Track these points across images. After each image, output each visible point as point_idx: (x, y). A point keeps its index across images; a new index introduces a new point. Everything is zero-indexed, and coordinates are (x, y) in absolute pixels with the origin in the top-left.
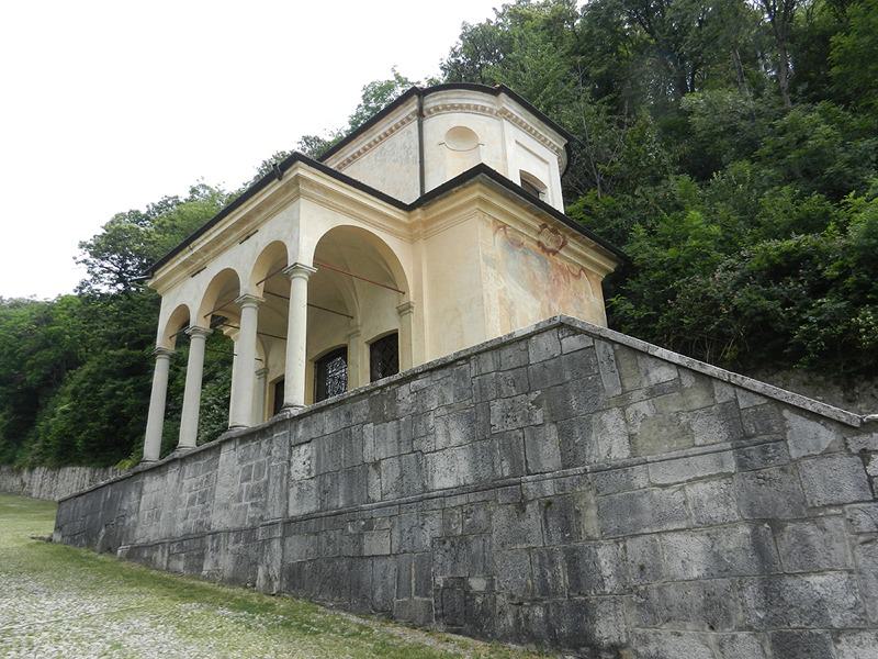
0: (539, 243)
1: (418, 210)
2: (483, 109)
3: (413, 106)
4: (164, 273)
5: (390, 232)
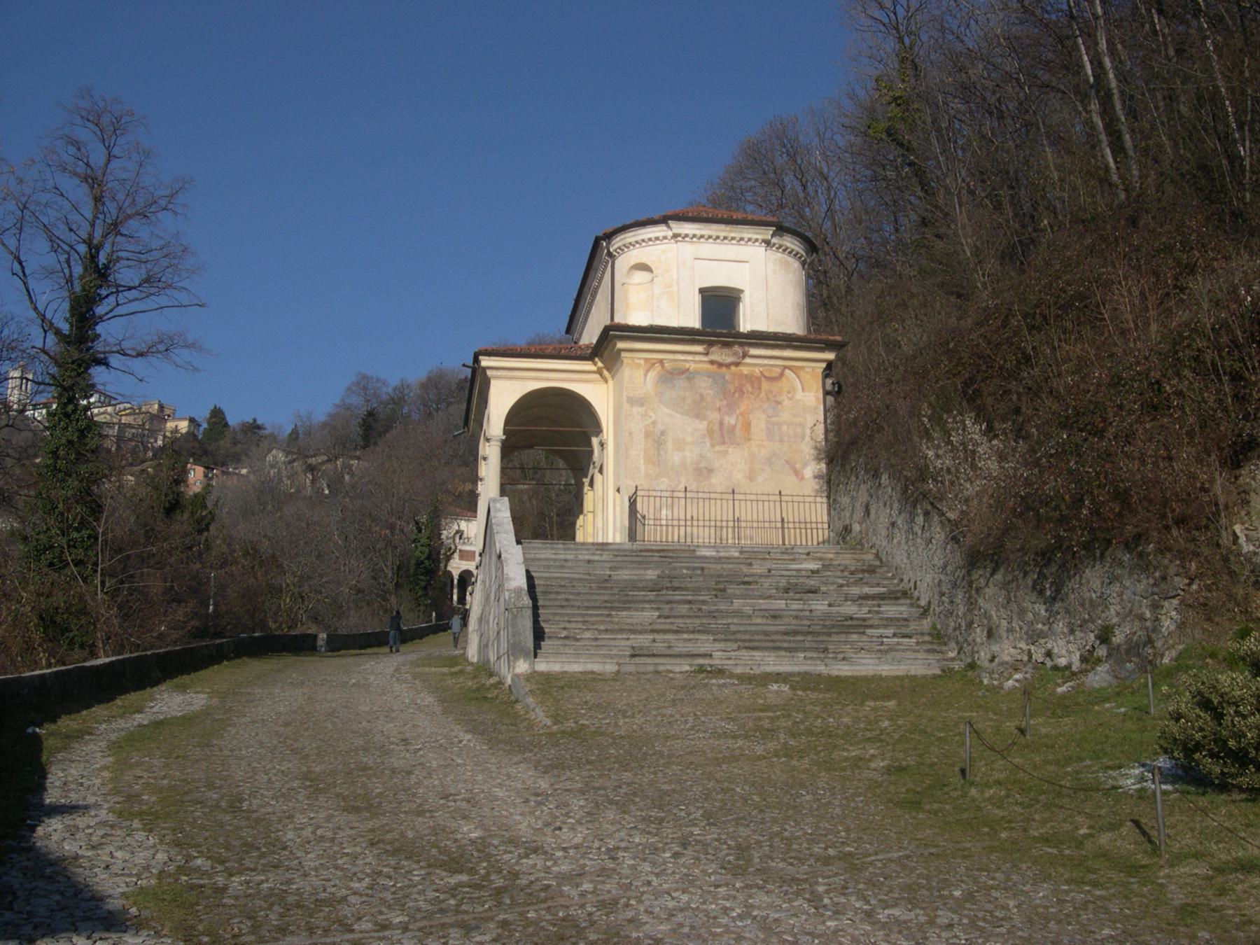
0: (712, 362)
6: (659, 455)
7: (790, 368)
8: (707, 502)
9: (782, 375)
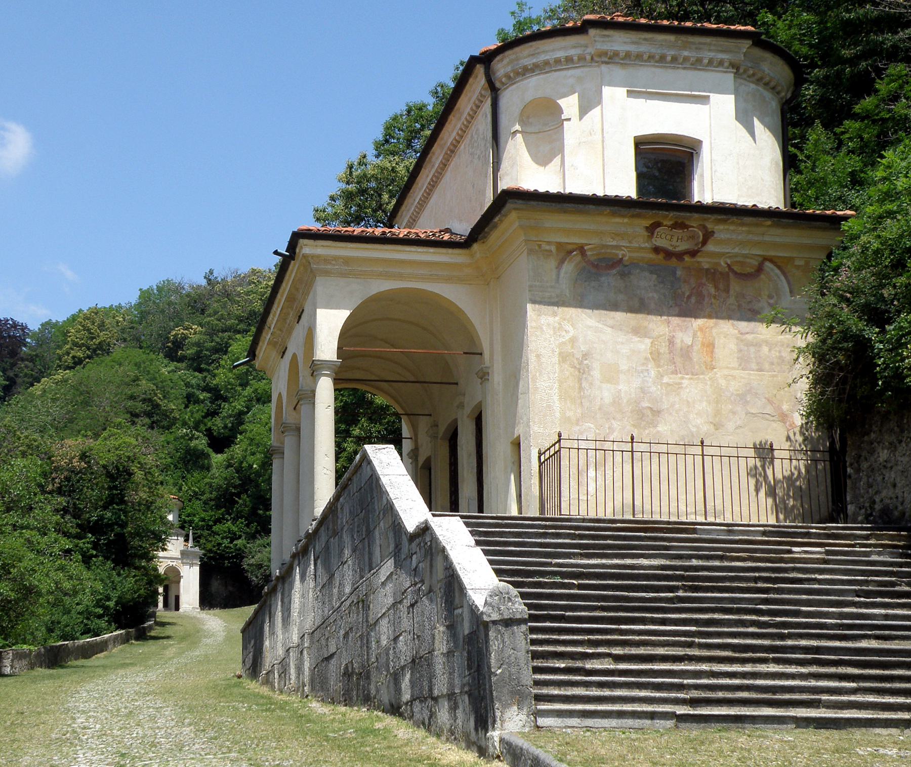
1: (475, 246)
2: (569, 60)
3: (478, 82)
5: (449, 280)
7: (771, 260)
8: (664, 458)
9: (760, 269)
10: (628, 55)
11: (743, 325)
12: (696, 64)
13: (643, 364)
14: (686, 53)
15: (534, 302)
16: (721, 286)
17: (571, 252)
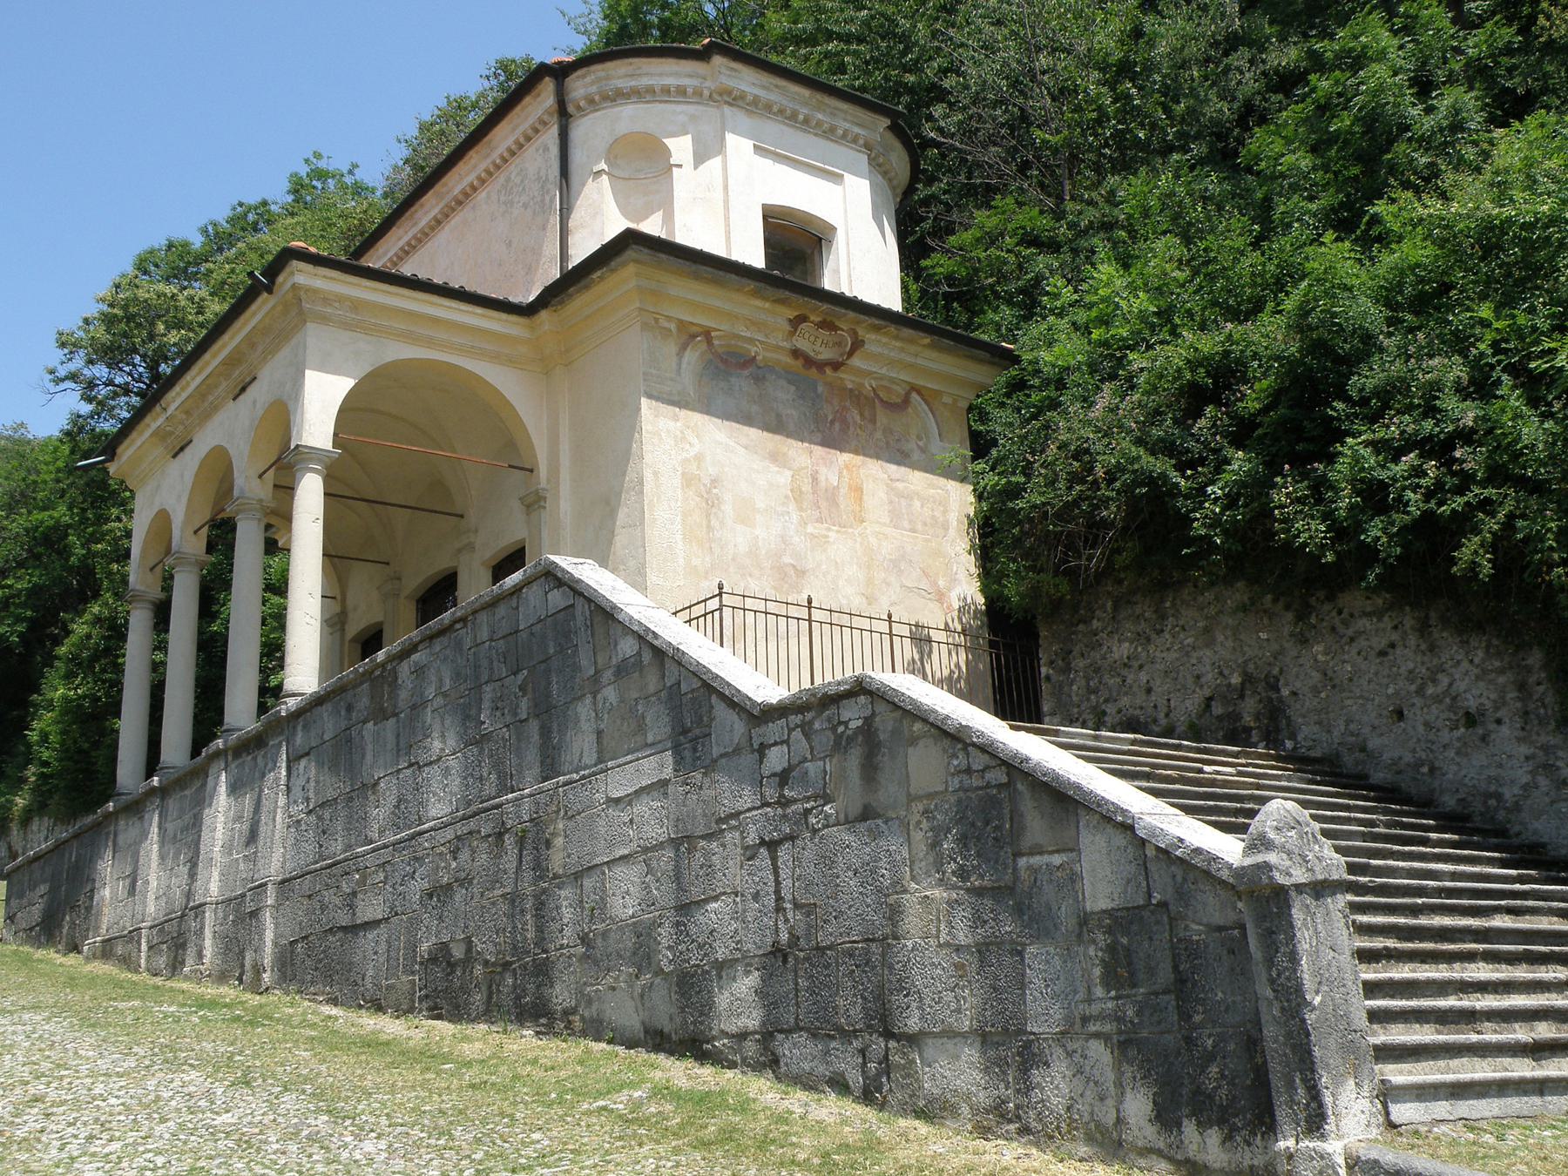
1: (544, 315)
2: (681, 91)
3: (544, 98)
4: (134, 447)
5: (495, 358)
6: (710, 528)
8: (846, 631)
9: (906, 401)
10: (756, 101)
11: (893, 467)
12: (829, 133)
13: (783, 504)
14: (820, 116)
15: (650, 397)
16: (866, 413)
17: (694, 336)
